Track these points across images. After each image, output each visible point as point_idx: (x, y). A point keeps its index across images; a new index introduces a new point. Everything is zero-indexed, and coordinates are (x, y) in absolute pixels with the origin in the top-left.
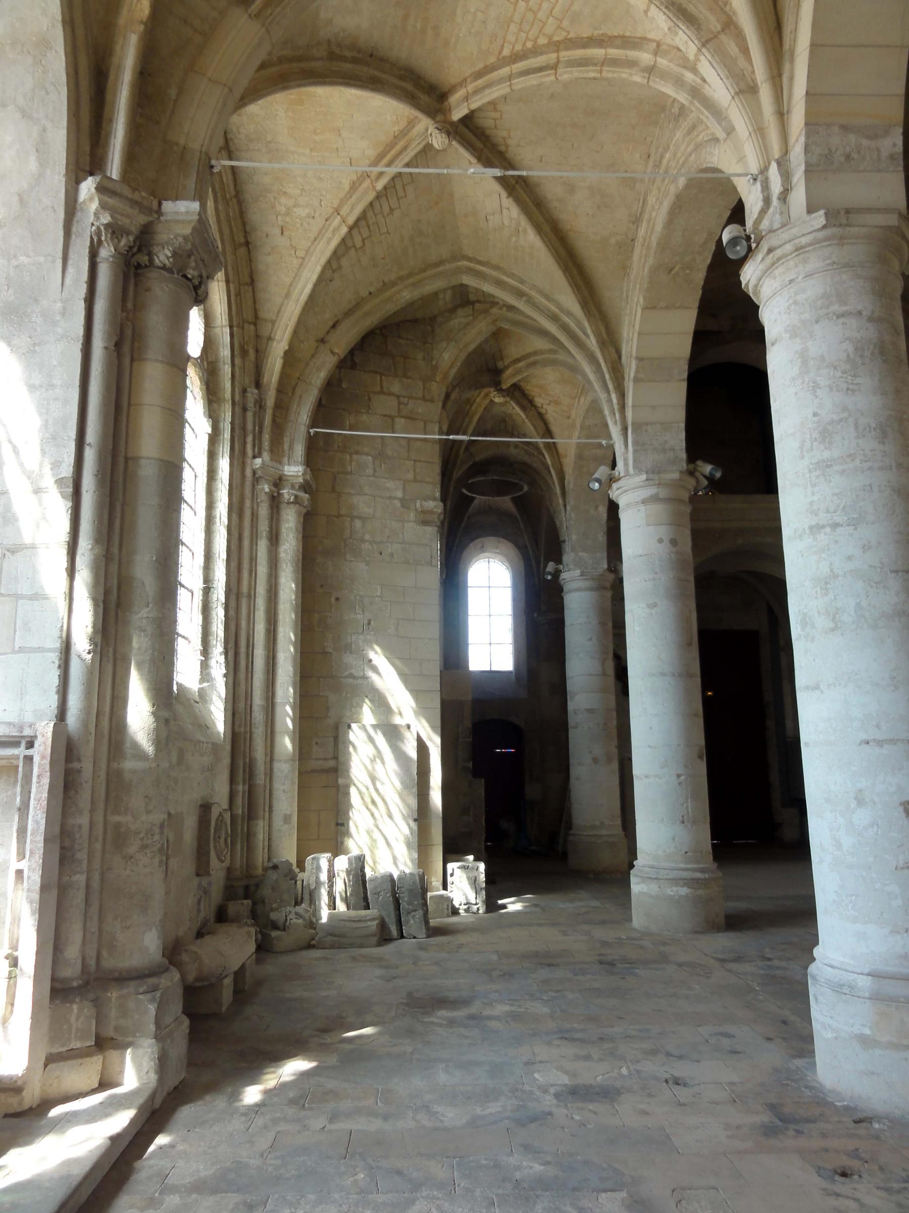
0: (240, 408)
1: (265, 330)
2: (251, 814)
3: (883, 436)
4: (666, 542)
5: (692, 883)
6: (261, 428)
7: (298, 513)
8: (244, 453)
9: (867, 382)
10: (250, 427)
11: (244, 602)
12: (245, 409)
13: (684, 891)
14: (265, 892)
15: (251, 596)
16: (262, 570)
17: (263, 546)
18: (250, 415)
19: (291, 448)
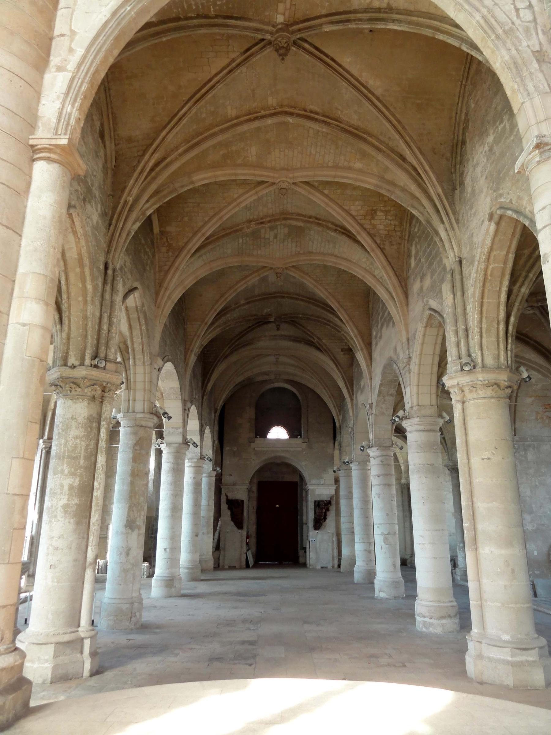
5: (188, 568)
9: (170, 475)
13: (186, 571)
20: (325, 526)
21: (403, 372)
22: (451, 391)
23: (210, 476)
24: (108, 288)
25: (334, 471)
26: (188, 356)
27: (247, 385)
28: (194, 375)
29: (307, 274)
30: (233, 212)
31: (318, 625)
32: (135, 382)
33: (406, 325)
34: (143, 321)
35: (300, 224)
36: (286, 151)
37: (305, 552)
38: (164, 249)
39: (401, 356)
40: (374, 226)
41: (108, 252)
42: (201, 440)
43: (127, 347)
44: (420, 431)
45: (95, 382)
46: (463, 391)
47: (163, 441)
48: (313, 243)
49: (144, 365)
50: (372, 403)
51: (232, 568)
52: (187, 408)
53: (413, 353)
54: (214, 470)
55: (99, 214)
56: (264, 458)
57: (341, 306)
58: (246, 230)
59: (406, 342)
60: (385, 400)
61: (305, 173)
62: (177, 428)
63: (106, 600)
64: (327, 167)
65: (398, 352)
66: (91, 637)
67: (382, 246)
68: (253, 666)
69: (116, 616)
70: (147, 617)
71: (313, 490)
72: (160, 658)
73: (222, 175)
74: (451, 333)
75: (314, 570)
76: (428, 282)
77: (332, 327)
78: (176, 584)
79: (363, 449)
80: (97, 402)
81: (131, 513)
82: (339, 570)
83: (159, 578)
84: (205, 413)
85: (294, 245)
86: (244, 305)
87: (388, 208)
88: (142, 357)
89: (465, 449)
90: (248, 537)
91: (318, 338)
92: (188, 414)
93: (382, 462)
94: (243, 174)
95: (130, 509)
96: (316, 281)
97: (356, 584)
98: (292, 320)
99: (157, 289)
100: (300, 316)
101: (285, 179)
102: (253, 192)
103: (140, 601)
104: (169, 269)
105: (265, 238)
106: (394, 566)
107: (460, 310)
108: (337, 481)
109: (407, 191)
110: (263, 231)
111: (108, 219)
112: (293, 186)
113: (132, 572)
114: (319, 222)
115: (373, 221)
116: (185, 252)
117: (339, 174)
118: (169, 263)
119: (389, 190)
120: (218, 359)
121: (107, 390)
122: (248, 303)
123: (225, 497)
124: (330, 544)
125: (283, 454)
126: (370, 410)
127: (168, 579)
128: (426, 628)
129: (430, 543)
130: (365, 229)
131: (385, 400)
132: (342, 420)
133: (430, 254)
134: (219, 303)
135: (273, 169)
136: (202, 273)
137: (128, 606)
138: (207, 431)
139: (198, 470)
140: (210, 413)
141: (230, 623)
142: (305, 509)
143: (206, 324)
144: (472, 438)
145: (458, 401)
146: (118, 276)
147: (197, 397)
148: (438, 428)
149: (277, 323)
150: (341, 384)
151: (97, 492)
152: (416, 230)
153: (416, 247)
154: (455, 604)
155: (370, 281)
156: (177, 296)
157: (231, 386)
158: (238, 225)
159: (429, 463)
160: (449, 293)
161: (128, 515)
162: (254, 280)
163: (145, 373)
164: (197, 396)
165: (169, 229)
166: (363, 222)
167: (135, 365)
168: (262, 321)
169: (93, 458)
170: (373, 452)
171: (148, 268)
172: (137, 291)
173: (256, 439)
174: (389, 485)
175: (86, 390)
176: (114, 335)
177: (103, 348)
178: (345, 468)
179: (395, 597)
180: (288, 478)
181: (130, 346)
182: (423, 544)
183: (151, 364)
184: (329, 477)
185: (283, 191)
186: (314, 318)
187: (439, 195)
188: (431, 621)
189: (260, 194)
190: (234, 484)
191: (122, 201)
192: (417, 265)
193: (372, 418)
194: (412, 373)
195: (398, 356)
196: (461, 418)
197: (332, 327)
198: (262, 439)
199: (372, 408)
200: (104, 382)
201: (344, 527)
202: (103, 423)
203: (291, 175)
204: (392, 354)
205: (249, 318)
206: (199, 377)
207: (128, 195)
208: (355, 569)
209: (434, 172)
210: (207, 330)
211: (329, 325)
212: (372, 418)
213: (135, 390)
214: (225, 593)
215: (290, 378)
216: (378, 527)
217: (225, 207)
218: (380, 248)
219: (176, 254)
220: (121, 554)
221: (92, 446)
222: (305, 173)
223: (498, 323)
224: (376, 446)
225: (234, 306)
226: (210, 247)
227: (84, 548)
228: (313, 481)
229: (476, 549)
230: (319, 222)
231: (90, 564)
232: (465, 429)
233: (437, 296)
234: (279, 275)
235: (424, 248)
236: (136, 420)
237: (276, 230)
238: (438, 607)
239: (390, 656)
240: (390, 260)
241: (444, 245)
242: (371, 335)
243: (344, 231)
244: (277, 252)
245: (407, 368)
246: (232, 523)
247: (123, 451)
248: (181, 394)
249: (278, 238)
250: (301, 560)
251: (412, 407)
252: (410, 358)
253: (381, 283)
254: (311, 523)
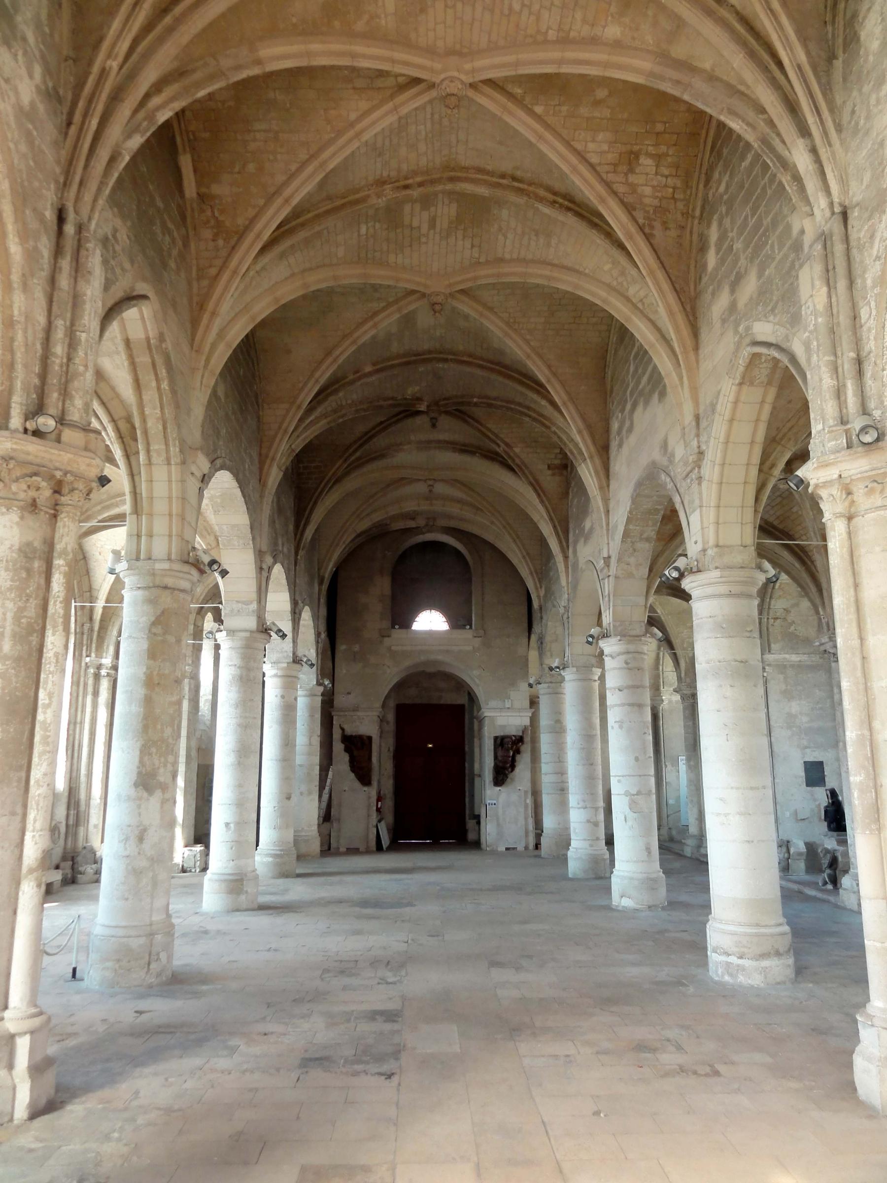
0: (80, 634)
1: (95, 594)
2: (77, 824)
3: (237, 707)
4: (279, 696)
5: (275, 856)
6: (91, 640)
7: (110, 681)
8: (81, 655)
10: (85, 642)
11: (78, 726)
12: (83, 634)
13: (270, 859)
14: (79, 859)
15: (82, 723)
16: (89, 709)
17: (89, 699)
18: (85, 637)
19: (108, 646)
20: (513, 780)
21: (683, 486)
22: (823, 493)
23: (312, 695)
24: (65, 263)
25: (531, 686)
26: (266, 467)
27: (378, 535)
28: (279, 509)
29: (491, 309)
30: (347, 152)
31: (518, 969)
32: (151, 498)
33: (695, 391)
34: (163, 372)
35: (482, 191)
36: (459, 5)
37: (479, 823)
38: (207, 234)
39: (679, 452)
40: (633, 188)
41: (66, 185)
42: (294, 628)
43: (133, 428)
44: (720, 596)
45: (35, 468)
46: (849, 493)
47: (222, 627)
48: (506, 237)
49: (169, 464)
50: (609, 557)
51: (353, 851)
52: (265, 566)
53: (707, 442)
54: (319, 684)
55: (37, 87)
56: (407, 663)
57: (555, 374)
58: (373, 200)
59: (694, 423)
60: (635, 550)
61: (497, 60)
62: (247, 603)
63: (98, 930)
64: (546, 41)
65: (670, 449)
66: (32, 1033)
67: (647, 230)
68: (395, 1079)
69: (118, 961)
70: (185, 955)
71: (492, 719)
72: (197, 1061)
73: (323, 52)
74: (824, 369)
75: (494, 853)
76: (750, 286)
77: (534, 419)
78: (250, 888)
79: (592, 640)
80: (44, 517)
81: (146, 758)
82: (536, 852)
83: (216, 877)
84: (302, 581)
85: (468, 244)
86: (370, 374)
87: (663, 148)
88: (163, 447)
89: (853, 617)
90: (379, 799)
91: (507, 444)
92: (268, 579)
93: (627, 663)
94: (369, 56)
95: (145, 751)
96: (507, 323)
97: (572, 880)
98: (459, 409)
99: (192, 312)
100: (475, 400)
101: (456, 74)
102: (390, 105)
103: (169, 929)
104: (218, 275)
105: (412, 228)
106: (648, 850)
107: (844, 319)
108: (534, 703)
109: (718, 79)
110: (407, 208)
111: (65, 110)
112: (471, 93)
113: (151, 874)
114: (521, 185)
115: (632, 178)
116: (251, 236)
117: (570, 55)
118: (218, 262)
119: (678, 82)
120: (325, 480)
121: (65, 490)
122: (378, 371)
123: (340, 731)
124: (522, 810)
125: (440, 657)
126: (605, 570)
127: (231, 877)
128: (731, 975)
129: (740, 814)
130: (615, 193)
131: (635, 550)
132: (545, 596)
133: (758, 225)
134: (324, 367)
135: (430, 51)
136: (289, 292)
137: (142, 940)
138: (306, 615)
139: (289, 682)
140: (310, 584)
141: (345, 968)
142: (477, 750)
143: (299, 407)
144: (870, 593)
145: (841, 515)
146: (88, 241)
147: (285, 550)
148: (755, 590)
149: (433, 415)
150: (546, 529)
151: (45, 713)
152: (722, 188)
153: (720, 224)
154: (787, 928)
155: (619, 310)
156: (237, 333)
157: (348, 537)
158: (358, 191)
159: (739, 658)
160: (818, 283)
161: (141, 761)
162: (388, 321)
163: (170, 481)
164: (287, 548)
165: (216, 189)
166: (611, 177)
167: (150, 463)
168: (406, 411)
169: (34, 639)
170: (609, 646)
171: (172, 264)
172: (146, 302)
173: (393, 630)
174: (640, 706)
175: (14, 487)
176: (81, 368)
177: (55, 395)
178: (549, 680)
179: (649, 907)
180: (451, 698)
181: (137, 424)
182: (726, 815)
183: (183, 463)
184: (520, 696)
185: (452, 101)
186: (499, 403)
187: (799, 67)
188: (740, 962)
189: (404, 111)
190: (356, 709)
191: (96, 69)
192: (722, 261)
193: (608, 586)
194: (704, 484)
195: (673, 455)
196: (845, 551)
197: (534, 419)
198: (404, 631)
199: (608, 566)
200: (57, 469)
201: (547, 780)
202: (58, 562)
203: (468, 66)
204: (657, 455)
205: (382, 403)
206: (290, 514)
207: (109, 56)
208: (570, 854)
209: (790, 16)
210: (301, 420)
211: (530, 416)
212: (608, 586)
213: (151, 515)
214: (340, 902)
215: (453, 524)
216: (619, 781)
217: (331, 141)
218: (644, 234)
219: (233, 242)
220: (127, 839)
221: (32, 611)
222: (497, 60)
224: (616, 635)
225: (351, 377)
226: (302, 234)
227: (15, 836)
228: (493, 704)
229: (879, 830)
230: (521, 185)
231: (31, 871)
232: (855, 574)
233: (773, 310)
234: (437, 307)
235: (739, 222)
236: (153, 574)
237: (433, 209)
238: (757, 935)
239: (679, 1048)
240: (662, 258)
241: (802, 189)
242: (607, 431)
243: (570, 205)
244: (434, 259)
245: (693, 476)
246: (352, 775)
247: (130, 637)
248: (254, 539)
249: (438, 230)
250: (471, 836)
251: (704, 550)
252: (701, 453)
253: (641, 312)
254: (488, 774)
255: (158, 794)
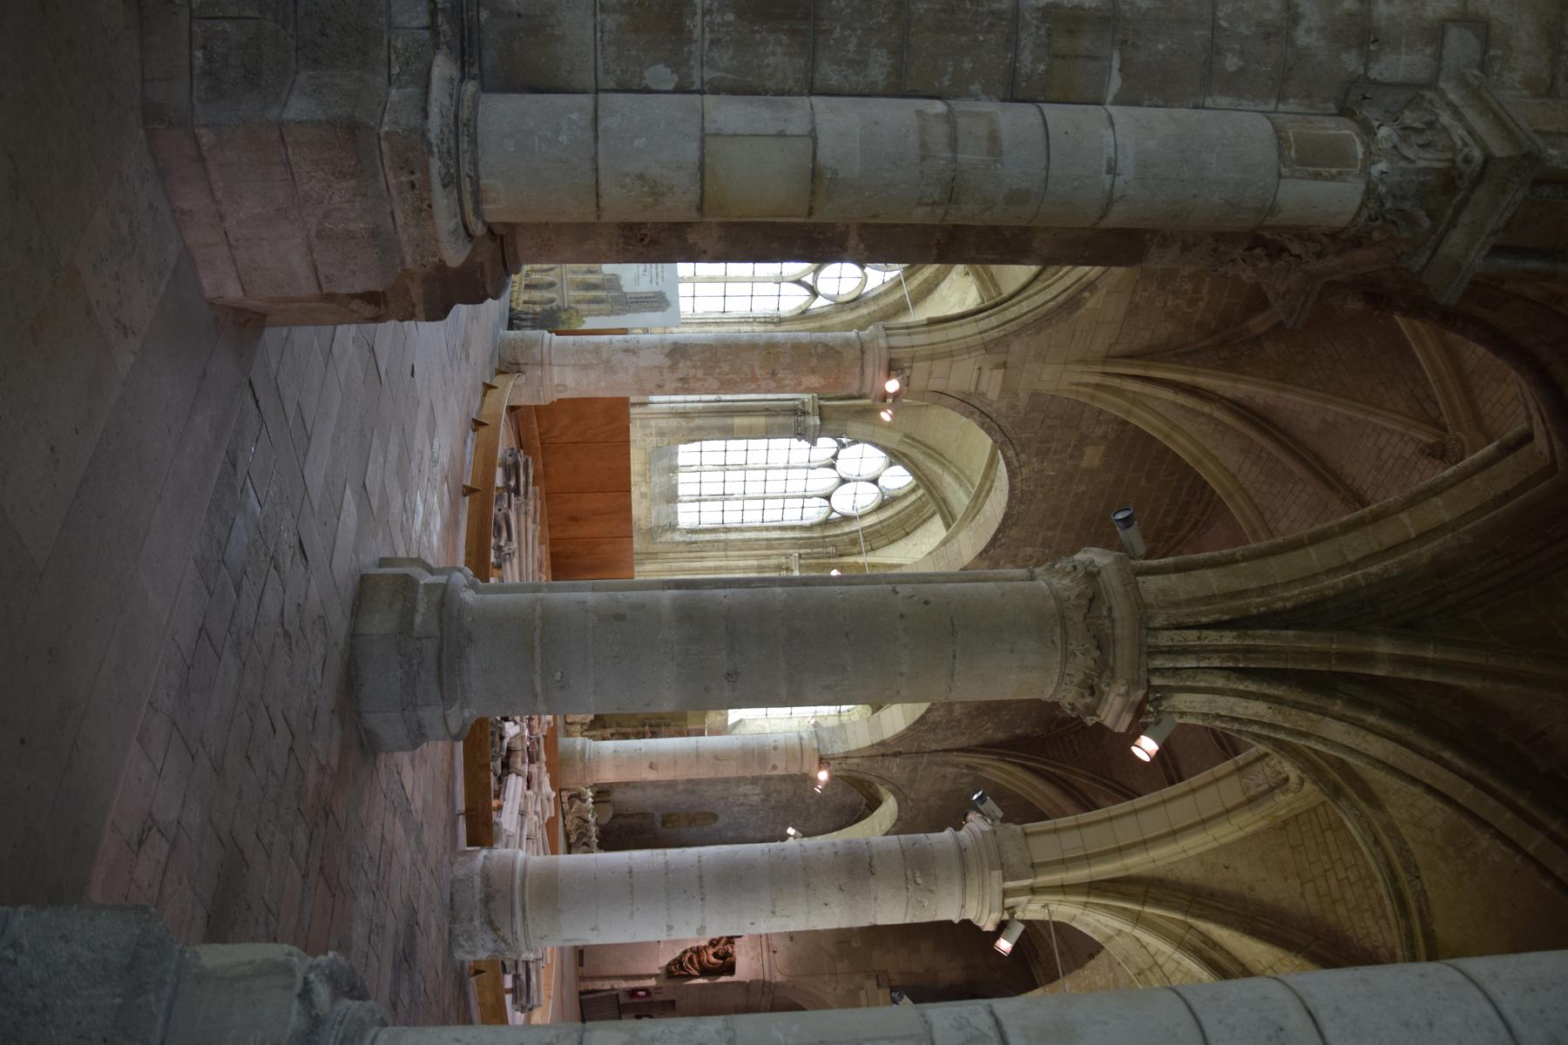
0: (822, 542)
8: (801, 547)
16: (741, 563)
161: (696, 345)
223: (1262, 590)
226: (1268, 445)
238: (513, 870)
255: (668, 362)
